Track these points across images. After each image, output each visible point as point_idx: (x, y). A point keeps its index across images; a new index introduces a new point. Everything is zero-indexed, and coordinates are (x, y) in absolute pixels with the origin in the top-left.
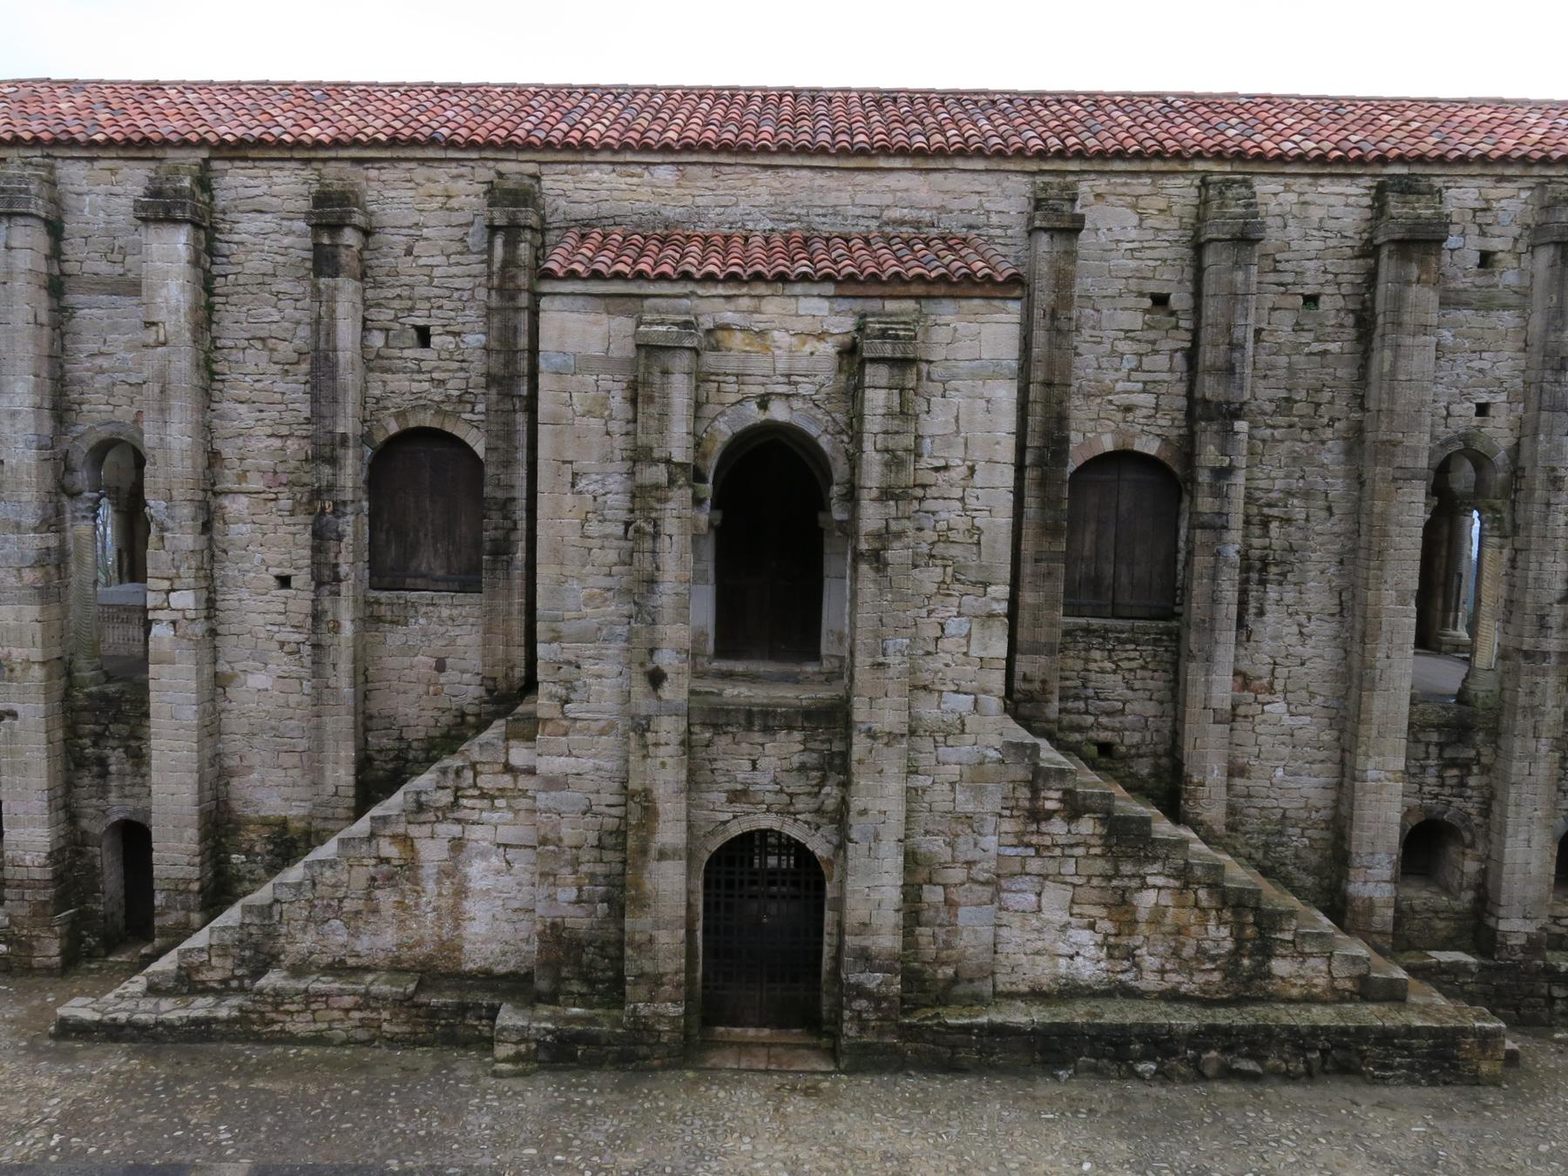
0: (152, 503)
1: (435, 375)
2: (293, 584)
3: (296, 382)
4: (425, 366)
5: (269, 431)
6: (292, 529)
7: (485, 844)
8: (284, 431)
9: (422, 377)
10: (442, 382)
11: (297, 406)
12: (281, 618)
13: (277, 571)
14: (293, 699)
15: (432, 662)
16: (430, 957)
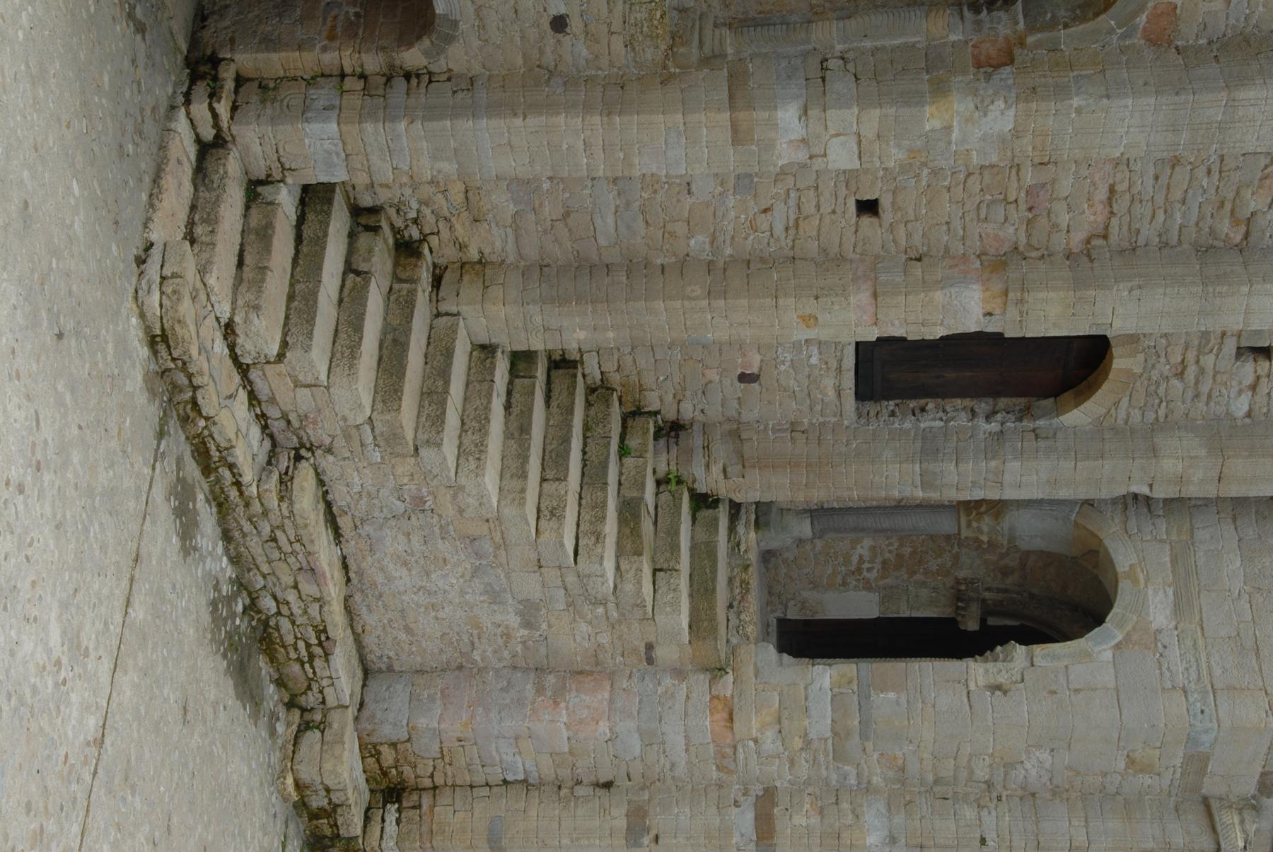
0: (1011, 112)
1: (1191, 371)
2: (866, 220)
3: (1201, 218)
4: (1209, 361)
5: (1119, 188)
6: (957, 224)
7: (544, 626)
8: (1121, 206)
9: (1191, 356)
10: (1180, 375)
11: (1161, 217)
12: (809, 208)
13: (885, 203)
14: (681, 229)
15: (754, 370)
16: (374, 585)
